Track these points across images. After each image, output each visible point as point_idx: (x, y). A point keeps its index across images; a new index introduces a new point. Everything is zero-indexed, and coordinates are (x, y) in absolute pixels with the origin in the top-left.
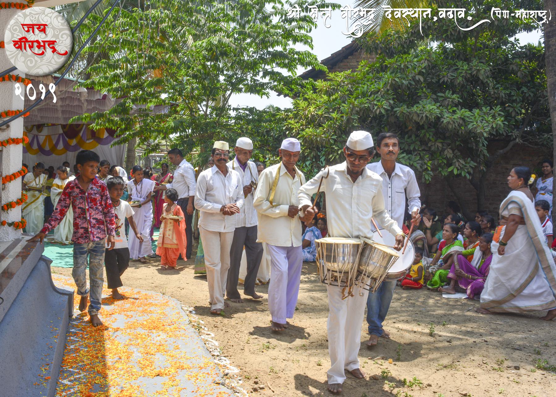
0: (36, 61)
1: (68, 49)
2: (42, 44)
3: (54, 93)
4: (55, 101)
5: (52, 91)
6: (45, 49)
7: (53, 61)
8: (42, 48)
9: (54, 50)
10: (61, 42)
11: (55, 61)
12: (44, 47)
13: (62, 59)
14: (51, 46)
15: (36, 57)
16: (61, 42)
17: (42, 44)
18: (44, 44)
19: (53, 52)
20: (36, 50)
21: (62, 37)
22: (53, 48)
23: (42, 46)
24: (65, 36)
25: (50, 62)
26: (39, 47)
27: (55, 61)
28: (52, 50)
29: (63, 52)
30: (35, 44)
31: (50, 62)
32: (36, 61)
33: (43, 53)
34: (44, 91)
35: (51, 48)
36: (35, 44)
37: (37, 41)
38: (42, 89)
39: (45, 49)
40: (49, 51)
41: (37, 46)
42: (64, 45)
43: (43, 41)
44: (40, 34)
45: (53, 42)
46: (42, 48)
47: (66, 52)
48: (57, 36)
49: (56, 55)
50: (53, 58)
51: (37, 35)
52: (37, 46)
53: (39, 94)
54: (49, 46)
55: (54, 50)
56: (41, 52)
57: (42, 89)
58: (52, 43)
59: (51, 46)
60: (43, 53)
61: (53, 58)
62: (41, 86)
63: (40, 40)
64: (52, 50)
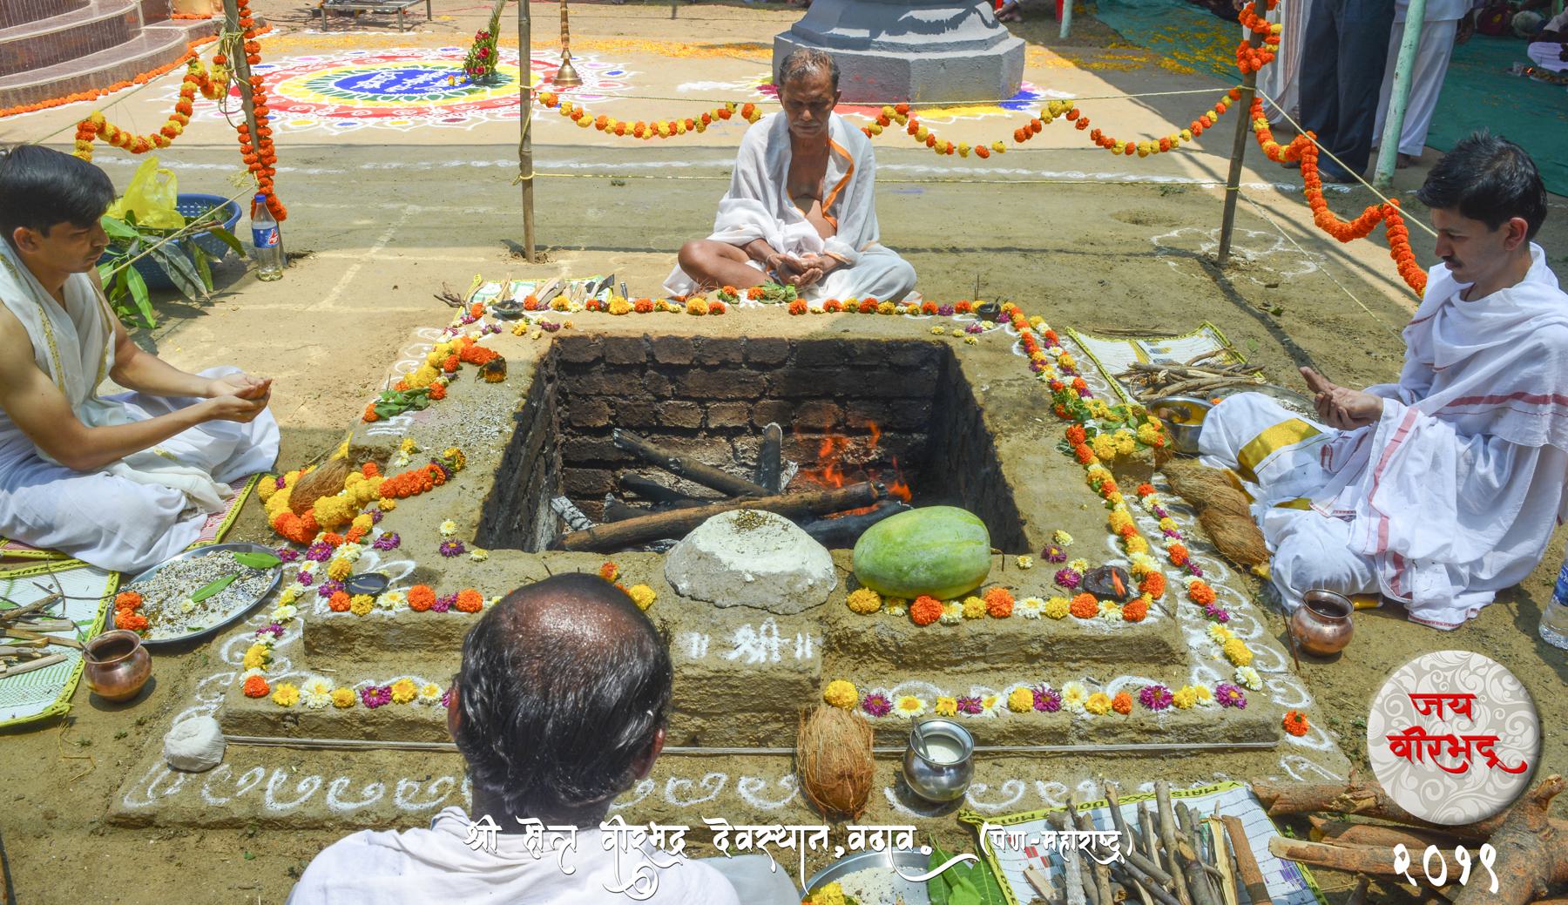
0: (1447, 788)
2: (1462, 744)
6: (1469, 756)
15: (1448, 779)
17: (1462, 744)
18: (1468, 745)
20: (1448, 760)
23: (1462, 749)
26: (1454, 752)
30: (1446, 745)
32: (1447, 788)
33: (1464, 768)
36: (1446, 745)
37: (1451, 738)
39: (1469, 756)
43: (1467, 739)
44: (1457, 720)
51: (1451, 722)
52: (1450, 751)
56: (1458, 765)
60: (1464, 768)
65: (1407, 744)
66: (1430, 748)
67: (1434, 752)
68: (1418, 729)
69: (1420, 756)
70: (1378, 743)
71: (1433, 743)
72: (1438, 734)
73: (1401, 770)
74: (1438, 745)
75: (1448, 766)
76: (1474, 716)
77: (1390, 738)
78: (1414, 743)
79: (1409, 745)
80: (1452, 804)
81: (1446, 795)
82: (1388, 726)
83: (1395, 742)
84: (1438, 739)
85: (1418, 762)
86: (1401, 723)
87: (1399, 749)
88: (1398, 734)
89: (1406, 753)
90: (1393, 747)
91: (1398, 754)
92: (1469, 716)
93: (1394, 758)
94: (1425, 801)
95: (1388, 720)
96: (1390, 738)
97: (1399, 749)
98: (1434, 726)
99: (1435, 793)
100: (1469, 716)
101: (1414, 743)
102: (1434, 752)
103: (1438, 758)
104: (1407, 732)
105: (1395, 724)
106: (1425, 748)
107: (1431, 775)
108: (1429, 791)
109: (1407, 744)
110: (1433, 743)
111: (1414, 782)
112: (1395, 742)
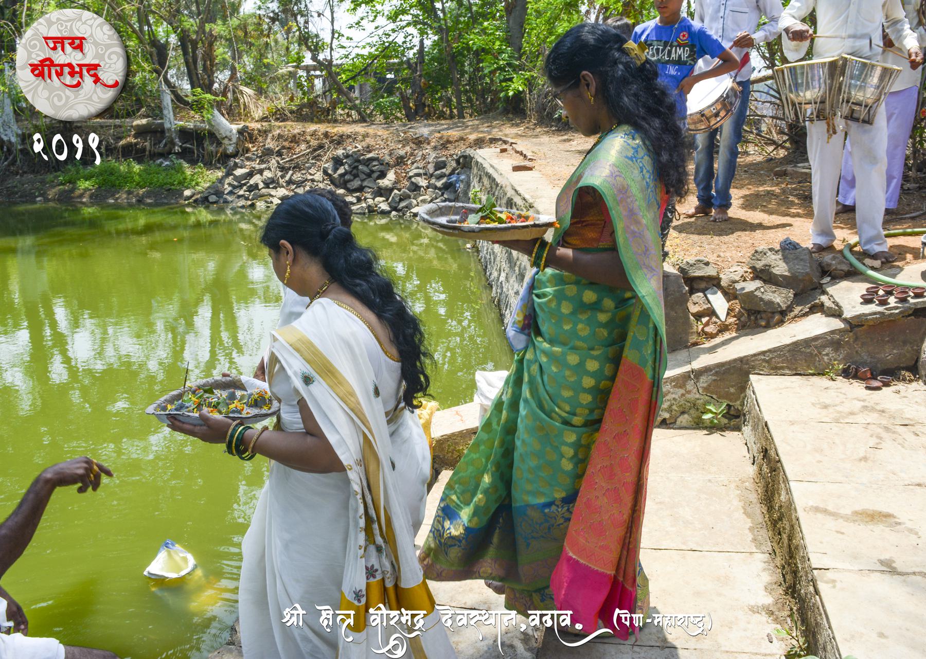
0: (68, 98)
1: (120, 78)
2: (77, 69)
3: (98, 148)
4: (98, 161)
5: (94, 145)
6: (81, 77)
7: (95, 98)
8: (77, 75)
9: (97, 80)
10: (107, 66)
11: (99, 98)
13: (110, 94)
14: (92, 72)
15: (68, 91)
16: (107, 66)
17: (77, 69)
18: (81, 70)
19: (95, 82)
20: (68, 80)
21: (110, 59)
22: (95, 75)
23: (77, 72)
24: (114, 57)
25: (90, 99)
26: (72, 74)
27: (99, 98)
28: (94, 79)
29: (111, 83)
30: (67, 70)
31: (90, 99)
32: (68, 98)
33: (78, 84)
34: (80, 146)
35: (91, 76)
36: (67, 70)
37: (70, 65)
38: (78, 142)
39: (81, 77)
40: (88, 80)
41: (69, 73)
42: (113, 71)
43: (80, 66)
45: (96, 67)
46: (77, 75)
47: (117, 84)
48: (102, 57)
49: (99, 88)
50: (95, 92)
52: (69, 73)
53: (72, 149)
54: (88, 71)
55: (97, 80)
56: (75, 83)
57: (78, 142)
58: (92, 68)
59: (92, 72)
60: (78, 84)
61: (95, 92)
62: (76, 137)
63: (74, 64)
64: (94, 79)
67: (59, 74)
71: (58, 68)
84: (62, 66)
98: (60, 58)
99: (60, 100)
102: (59, 74)
107: (58, 89)
110: (58, 68)
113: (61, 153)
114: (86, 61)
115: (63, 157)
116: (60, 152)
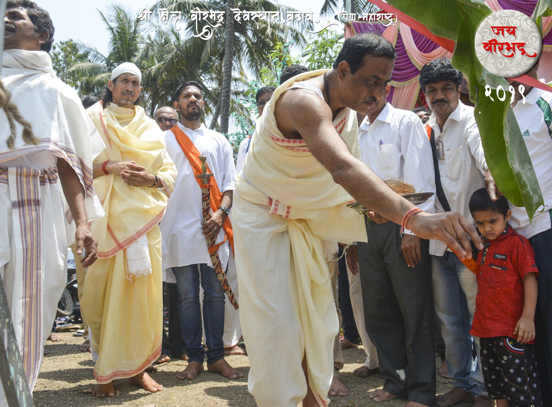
0: (506, 63)
2: (512, 46)
6: (514, 51)
8: (511, 50)
12: (514, 49)
15: (506, 60)
17: (512, 46)
18: (514, 46)
20: (506, 52)
23: (511, 48)
26: (509, 49)
30: (505, 46)
32: (506, 63)
33: (512, 55)
34: (513, 92)
36: (505, 46)
37: (507, 44)
38: (512, 90)
39: (514, 51)
41: (507, 48)
43: (513, 44)
44: (510, 36)
46: (511, 50)
51: (507, 37)
52: (507, 48)
56: (510, 54)
57: (512, 90)
60: (512, 55)
63: (510, 43)
65: (490, 46)
66: (499, 47)
67: (501, 49)
68: (495, 40)
69: (495, 51)
70: (479, 45)
71: (500, 46)
72: (502, 42)
73: (488, 56)
74: (502, 46)
75: (506, 55)
76: (516, 35)
77: (484, 44)
78: (493, 46)
79: (491, 46)
80: (507, 70)
81: (505, 66)
82: (483, 39)
83: (485, 45)
84: (502, 44)
85: (494, 53)
86: (488, 38)
87: (487, 48)
88: (487, 42)
89: (490, 49)
90: (485, 47)
91: (486, 50)
92: (514, 35)
93: (485, 51)
94: (497, 68)
95: (483, 36)
96: (484, 44)
97: (487, 48)
98: (501, 39)
99: (501, 64)
100: (514, 35)
101: (493, 46)
102: (501, 49)
103: (502, 51)
104: (490, 41)
105: (485, 38)
106: (497, 48)
108: (499, 64)
109: (490, 46)
110: (500, 46)
111: (493, 61)
112: (485, 45)
113: (501, 97)
114: (517, 41)
115: (503, 99)
116: (501, 96)
